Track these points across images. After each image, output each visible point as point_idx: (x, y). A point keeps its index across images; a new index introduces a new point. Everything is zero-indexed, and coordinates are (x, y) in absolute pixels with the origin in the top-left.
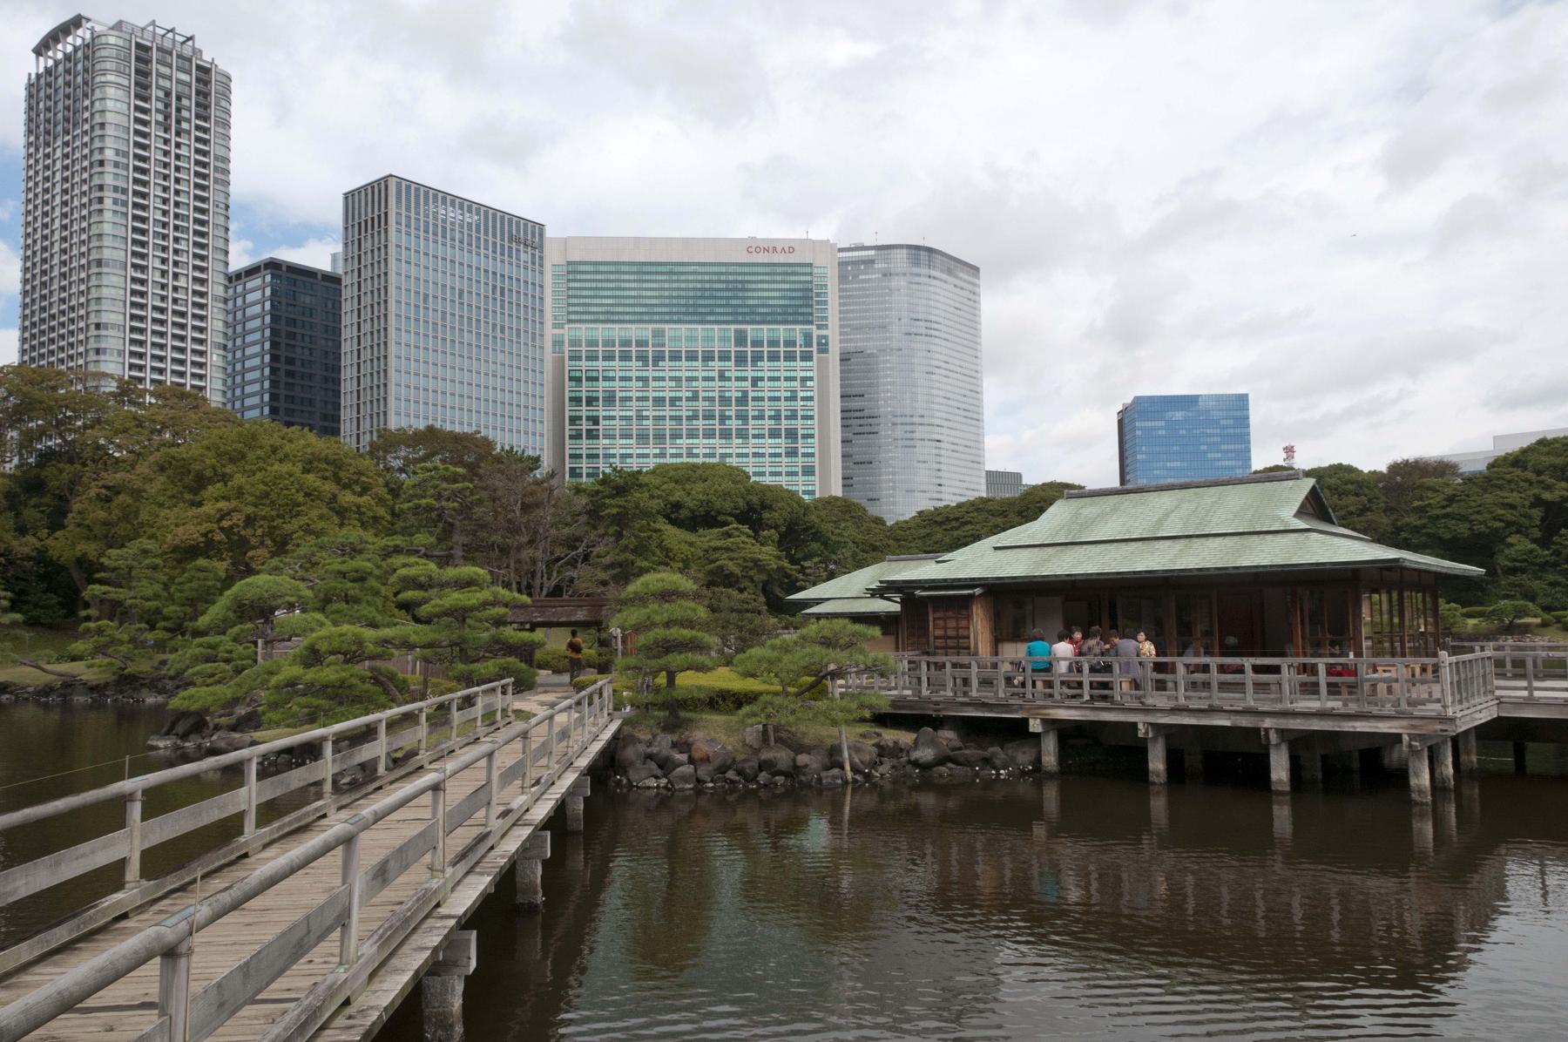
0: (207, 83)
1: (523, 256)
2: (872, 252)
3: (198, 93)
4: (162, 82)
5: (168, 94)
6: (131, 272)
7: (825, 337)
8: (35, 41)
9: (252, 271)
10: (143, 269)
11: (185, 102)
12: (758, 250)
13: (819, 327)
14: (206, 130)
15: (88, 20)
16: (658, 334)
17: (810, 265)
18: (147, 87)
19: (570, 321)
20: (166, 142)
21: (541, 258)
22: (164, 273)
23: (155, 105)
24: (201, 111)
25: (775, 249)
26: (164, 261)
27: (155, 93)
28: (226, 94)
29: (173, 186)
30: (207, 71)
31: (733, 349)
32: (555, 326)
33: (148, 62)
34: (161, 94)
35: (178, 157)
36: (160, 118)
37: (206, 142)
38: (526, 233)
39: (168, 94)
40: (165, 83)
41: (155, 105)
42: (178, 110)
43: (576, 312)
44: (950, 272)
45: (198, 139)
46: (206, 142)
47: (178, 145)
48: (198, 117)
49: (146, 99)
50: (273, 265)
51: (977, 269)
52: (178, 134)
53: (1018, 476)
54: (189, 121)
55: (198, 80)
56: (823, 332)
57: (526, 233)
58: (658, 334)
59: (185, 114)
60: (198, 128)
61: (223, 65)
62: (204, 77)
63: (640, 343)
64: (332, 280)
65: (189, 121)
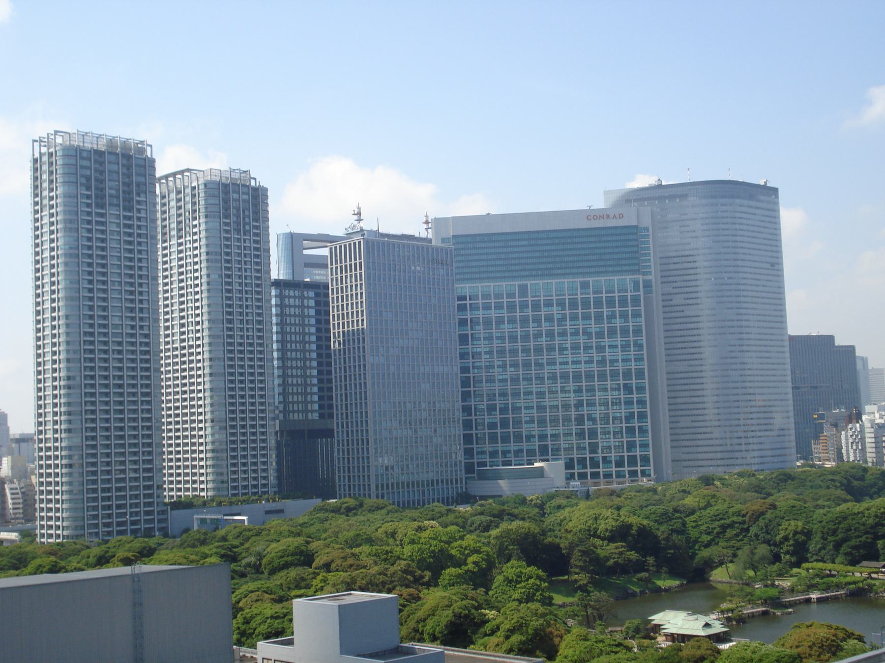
5: (238, 210)
7: (650, 281)
11: (247, 213)
12: (595, 217)
13: (644, 274)
16: (523, 290)
17: (636, 227)
23: (233, 219)
25: (608, 216)
27: (232, 211)
49: (226, 217)
51: (775, 191)
52: (245, 234)
53: (831, 338)
59: (247, 220)
63: (511, 295)
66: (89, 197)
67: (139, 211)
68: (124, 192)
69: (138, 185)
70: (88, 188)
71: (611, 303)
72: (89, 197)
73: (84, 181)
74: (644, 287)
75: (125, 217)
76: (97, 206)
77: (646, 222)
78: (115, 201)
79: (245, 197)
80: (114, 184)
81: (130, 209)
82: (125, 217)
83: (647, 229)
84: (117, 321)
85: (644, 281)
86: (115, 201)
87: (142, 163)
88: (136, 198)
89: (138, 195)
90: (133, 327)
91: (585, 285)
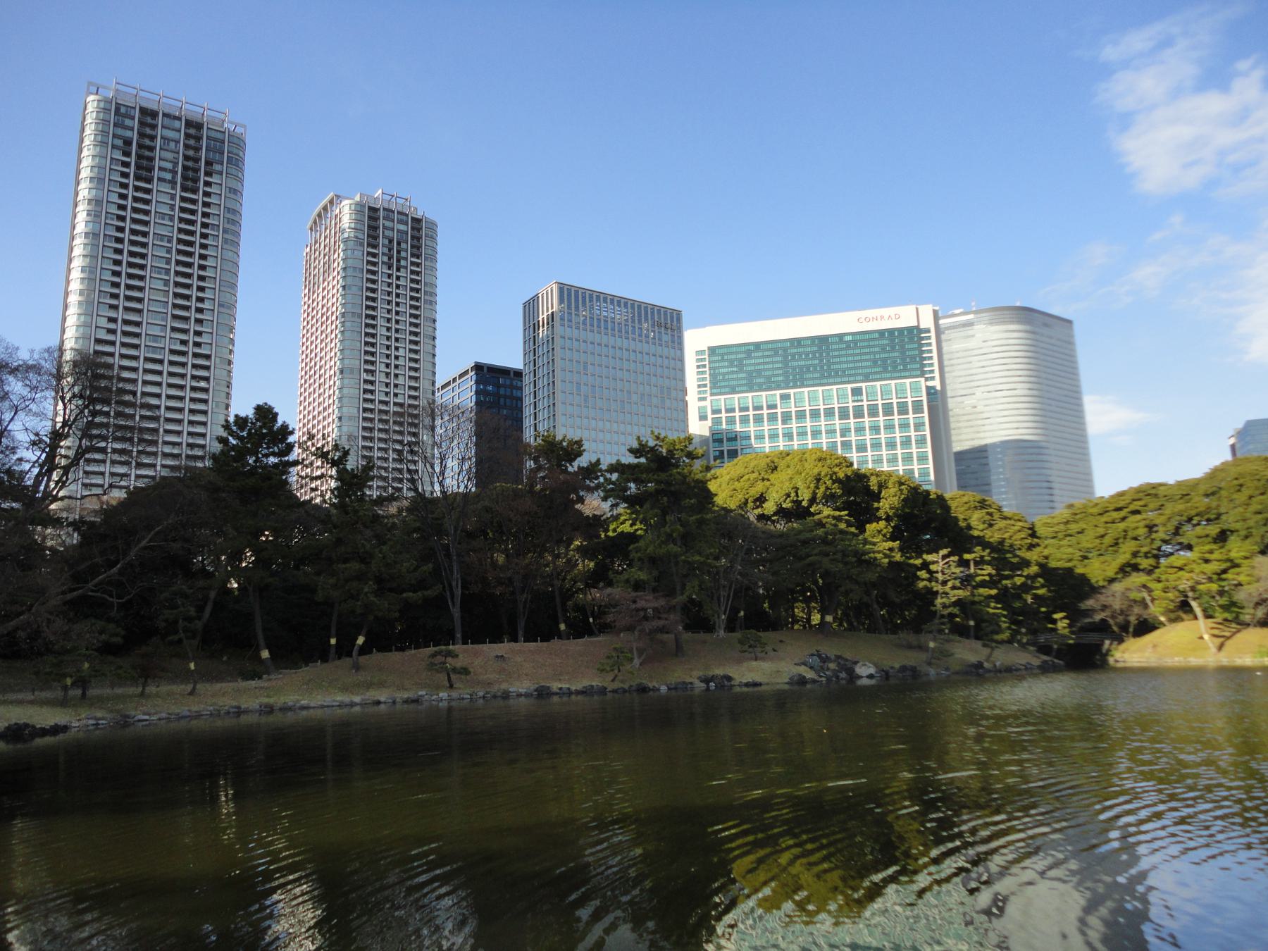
0: (419, 230)
1: (665, 338)
2: (971, 317)
3: (413, 238)
4: (387, 233)
5: (391, 241)
6: (365, 376)
8: (310, 223)
9: (466, 373)
10: (372, 372)
11: (403, 245)
13: (927, 379)
14: (418, 265)
15: (338, 197)
18: (376, 238)
19: (712, 394)
20: (390, 276)
22: (388, 374)
24: (415, 250)
25: (882, 317)
26: (388, 366)
28: (433, 238)
29: (394, 308)
30: (417, 221)
31: (851, 405)
32: (701, 399)
33: (377, 219)
34: (386, 242)
35: (398, 287)
36: (386, 259)
37: (418, 273)
38: (666, 319)
41: (381, 250)
42: (398, 252)
43: (718, 383)
44: (1046, 325)
45: (412, 272)
46: (418, 273)
47: (398, 278)
48: (412, 255)
49: (375, 247)
50: (478, 368)
51: (1070, 322)
52: (398, 270)
54: (406, 259)
55: (413, 228)
56: (930, 384)
57: (666, 319)
58: (785, 397)
59: (403, 254)
60: (413, 264)
61: (430, 215)
62: (417, 226)
64: (518, 374)
65: (406, 259)
66: (126, 164)
67: (207, 194)
68: (185, 168)
69: (209, 163)
70: (127, 154)
71: (888, 410)
72: (126, 164)
73: (119, 143)
74: (928, 394)
75: (183, 199)
76: (137, 178)
77: (927, 322)
78: (168, 176)
79: (402, 227)
80: (170, 156)
81: (195, 191)
82: (183, 199)
83: (928, 331)
84: (156, 331)
85: (928, 388)
86: (168, 176)
87: (219, 136)
89: (208, 174)
90: (184, 342)
91: (857, 392)
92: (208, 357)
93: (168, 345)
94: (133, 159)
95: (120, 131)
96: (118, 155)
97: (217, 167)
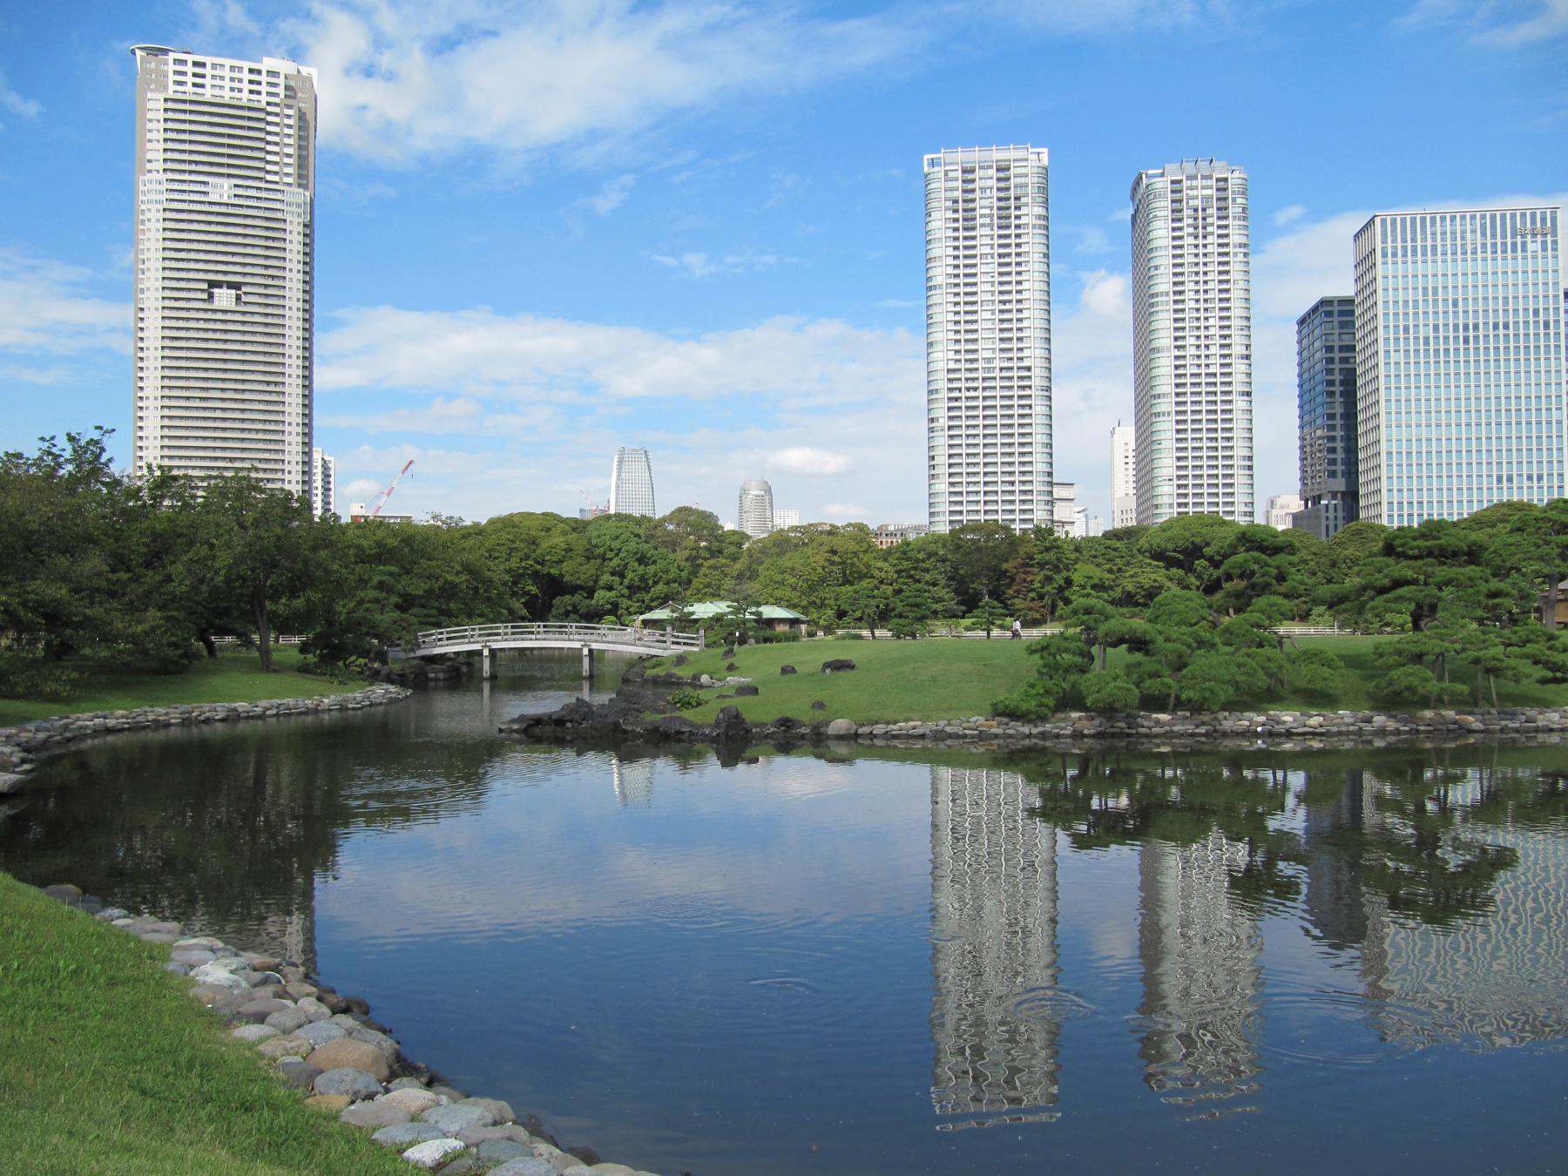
20: (1196, 246)
21: (1555, 242)
27: (1186, 212)
34: (1191, 212)
39: (1196, 210)
40: (1191, 203)
57: (1533, 222)
59: (1209, 220)
69: (1017, 198)
72: (956, 220)
73: (949, 204)
76: (965, 229)
78: (988, 221)
84: (989, 354)
86: (988, 221)
88: (1013, 212)
89: (1018, 208)
92: (1029, 369)
93: (997, 364)
94: (960, 215)
95: (949, 194)
96: (950, 215)
97: (1024, 200)
